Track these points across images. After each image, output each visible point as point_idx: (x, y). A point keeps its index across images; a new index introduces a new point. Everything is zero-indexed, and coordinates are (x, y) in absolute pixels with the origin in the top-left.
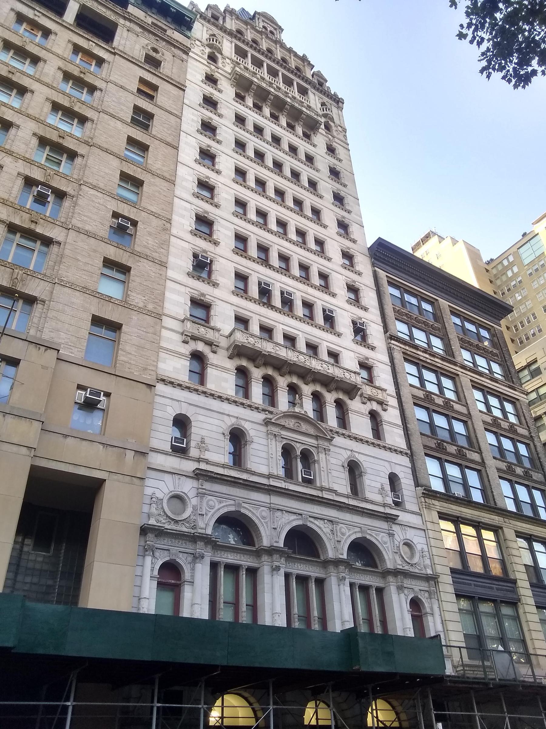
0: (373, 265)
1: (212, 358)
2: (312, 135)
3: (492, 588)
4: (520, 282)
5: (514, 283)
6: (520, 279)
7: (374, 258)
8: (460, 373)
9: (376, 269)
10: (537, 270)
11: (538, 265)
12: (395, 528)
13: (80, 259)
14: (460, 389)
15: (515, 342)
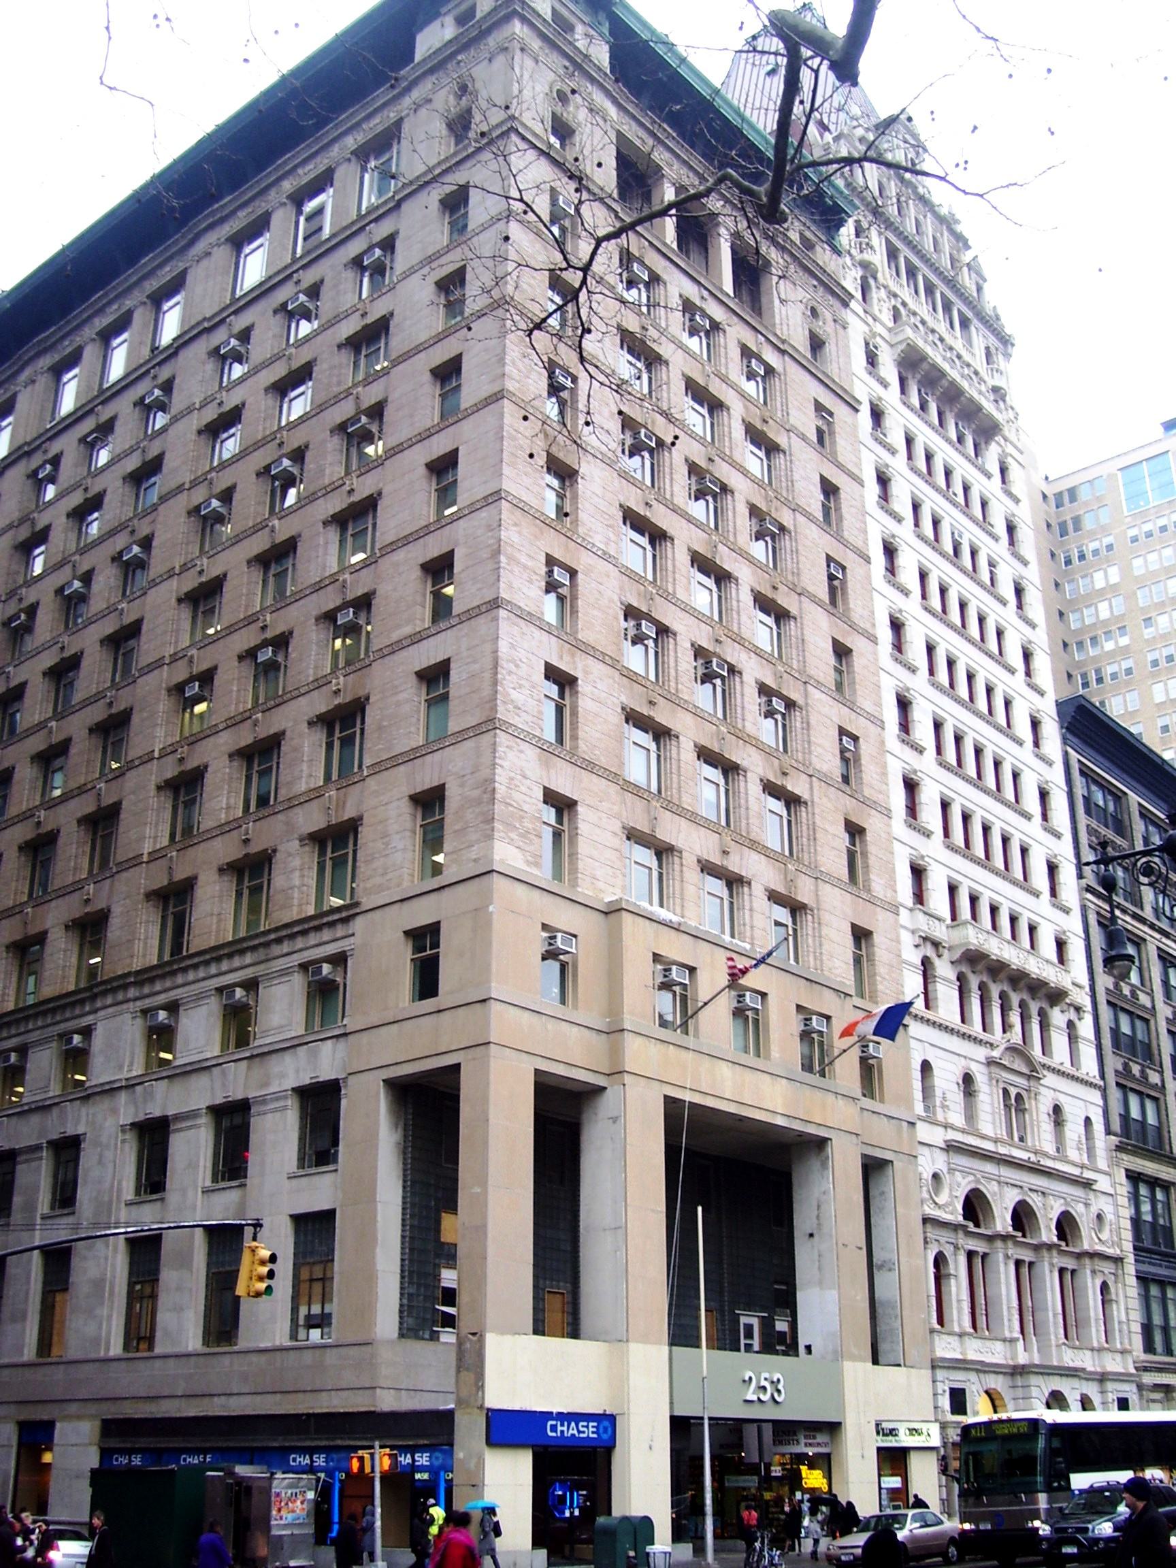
0: (1065, 741)
1: (937, 962)
2: (983, 446)
3: (1160, 1266)
4: (1110, 547)
5: (1093, 545)
6: (1107, 540)
7: (1067, 728)
8: (1148, 938)
9: (1070, 750)
10: (1149, 535)
11: (1155, 524)
12: (1091, 1195)
13: (827, 827)
14: (1145, 965)
15: (1074, 679)
